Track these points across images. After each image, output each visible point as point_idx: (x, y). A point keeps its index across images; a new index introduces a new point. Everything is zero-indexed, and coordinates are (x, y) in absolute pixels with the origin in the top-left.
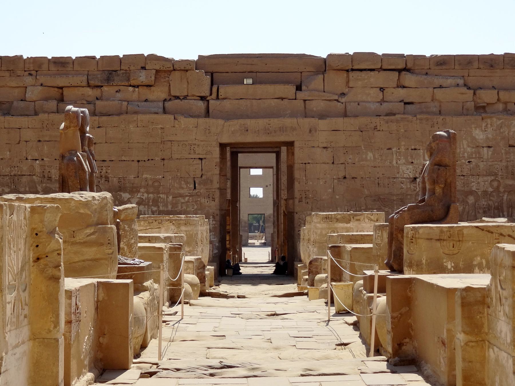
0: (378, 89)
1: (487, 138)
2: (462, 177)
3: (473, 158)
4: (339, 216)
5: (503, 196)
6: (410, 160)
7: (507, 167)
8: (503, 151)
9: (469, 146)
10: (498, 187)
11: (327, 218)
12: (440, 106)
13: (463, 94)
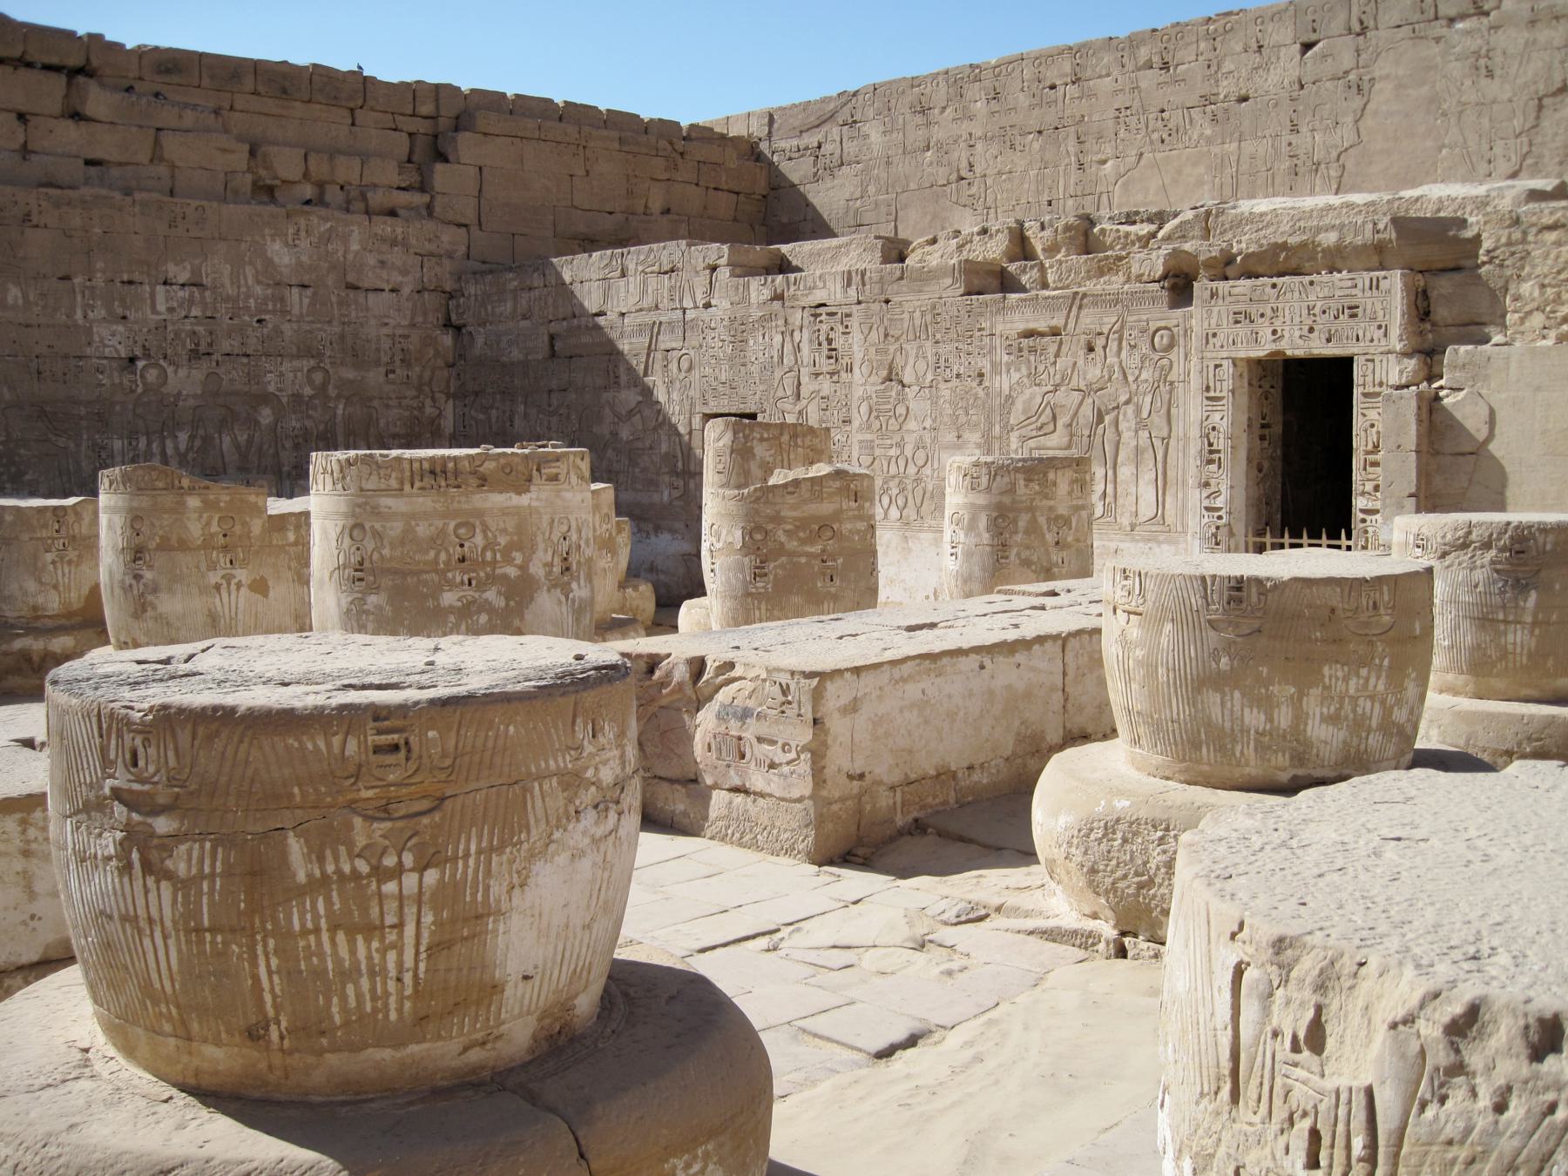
0: (14, 115)
1: (300, 264)
2: (245, 360)
3: (268, 312)
4: (490, 466)
5: (336, 407)
6: (120, 311)
7: (342, 337)
8: (334, 299)
9: (259, 282)
10: (324, 385)
11: (436, 471)
12: (173, 177)
13: (224, 150)
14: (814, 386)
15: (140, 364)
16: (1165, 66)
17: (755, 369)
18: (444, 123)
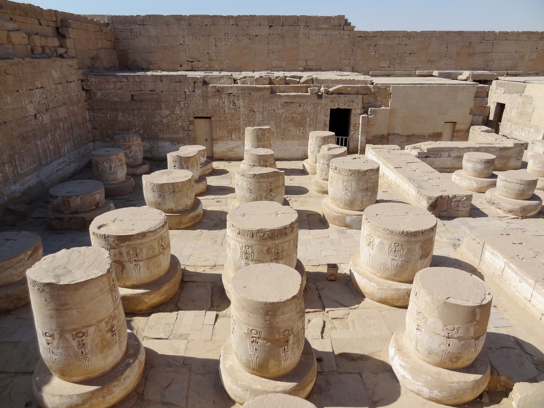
14: (229, 111)
15: (38, 116)
16: (237, 25)
17: (210, 107)
18: (59, 24)
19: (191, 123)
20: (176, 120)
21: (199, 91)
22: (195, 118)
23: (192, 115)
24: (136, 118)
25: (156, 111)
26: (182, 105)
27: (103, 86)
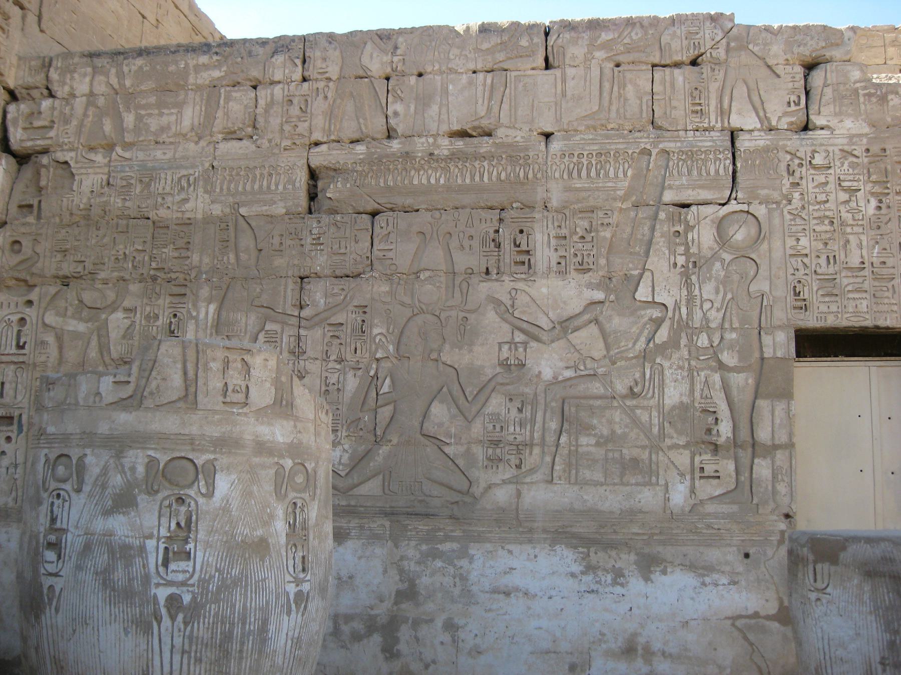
19: (771, 384)
20: (645, 356)
21: (850, 125)
22: (816, 344)
23: (780, 315)
24: (314, 338)
25: (484, 288)
26: (705, 237)
27: (129, 119)
